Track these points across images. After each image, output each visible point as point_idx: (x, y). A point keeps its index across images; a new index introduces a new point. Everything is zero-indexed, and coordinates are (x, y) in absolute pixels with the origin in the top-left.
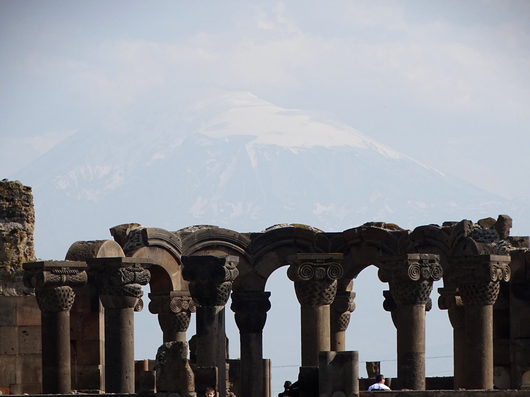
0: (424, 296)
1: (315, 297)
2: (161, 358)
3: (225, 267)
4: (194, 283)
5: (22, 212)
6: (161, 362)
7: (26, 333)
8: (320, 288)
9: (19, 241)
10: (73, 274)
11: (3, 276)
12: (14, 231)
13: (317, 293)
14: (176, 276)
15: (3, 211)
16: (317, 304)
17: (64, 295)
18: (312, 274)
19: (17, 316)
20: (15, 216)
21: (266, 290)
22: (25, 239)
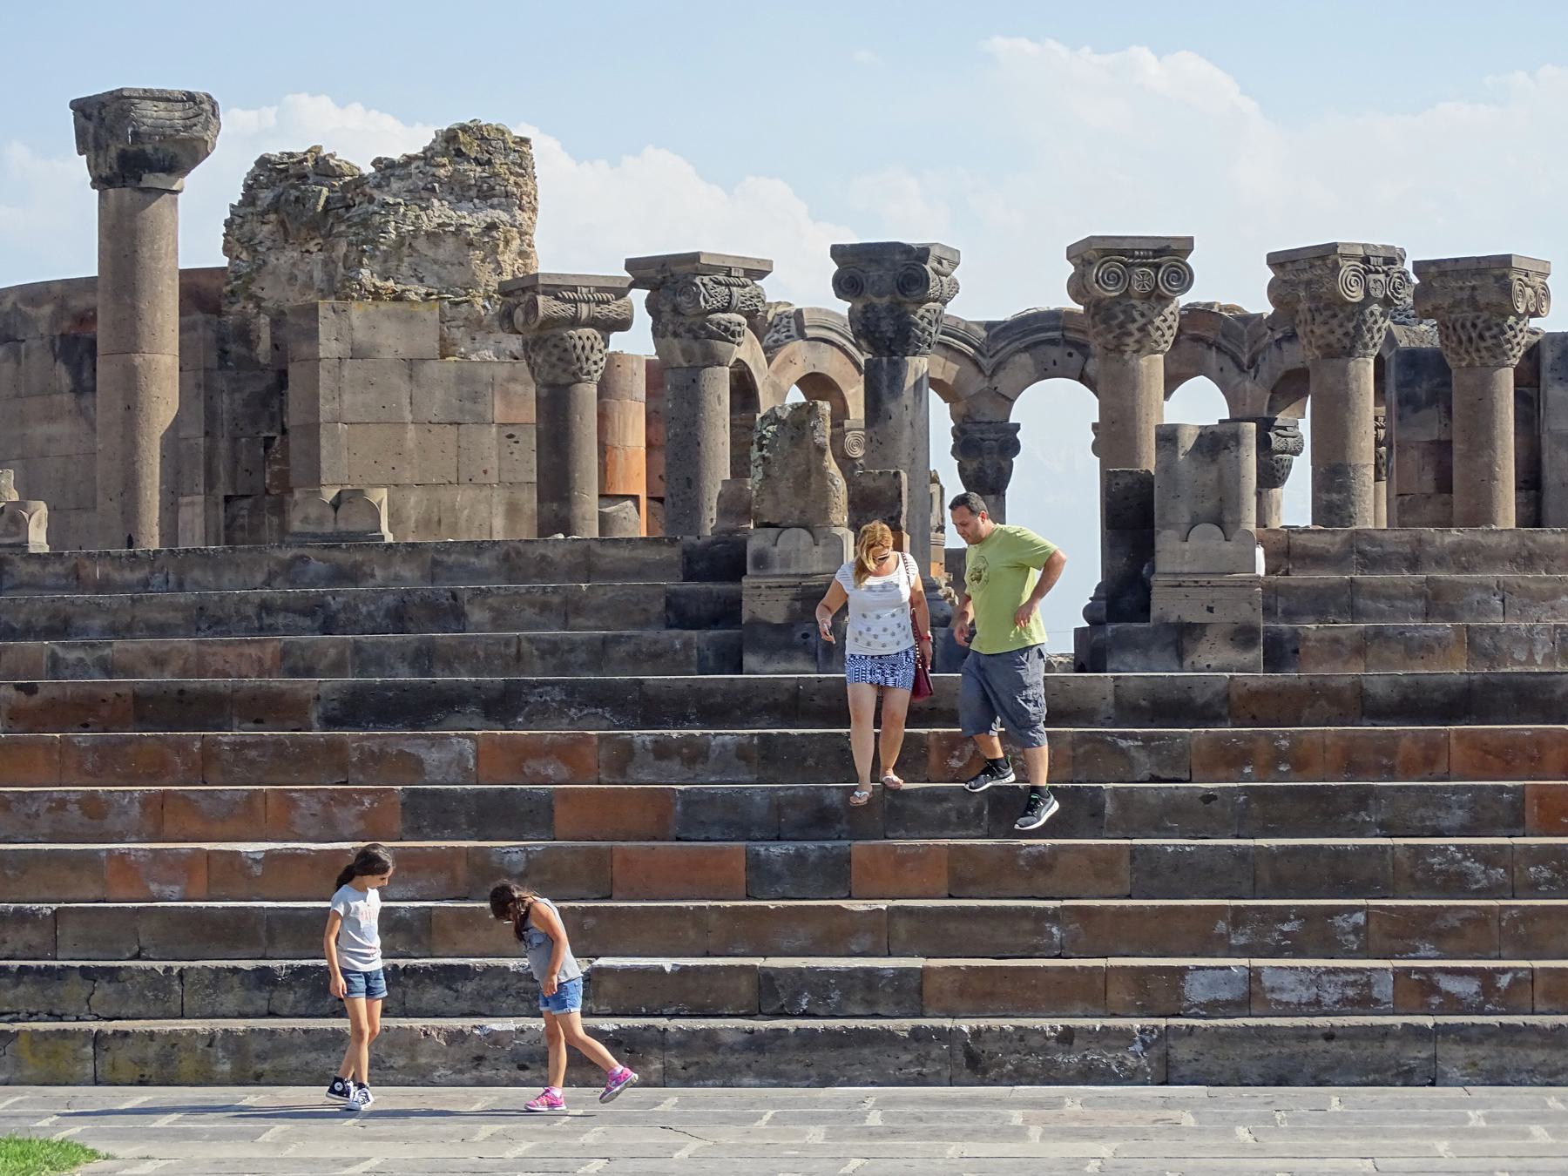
0: (1372, 338)
1: (1130, 334)
2: (764, 442)
3: (927, 267)
4: (860, 306)
5: (509, 188)
6: (764, 452)
7: (514, 439)
8: (1143, 315)
9: (501, 246)
10: (603, 302)
11: (466, 319)
12: (492, 227)
13: (1136, 325)
14: (855, 394)
15: (470, 185)
16: (1134, 352)
17: (583, 348)
18: (1125, 281)
19: (496, 402)
20: (495, 196)
21: (1012, 420)
22: (515, 244)
